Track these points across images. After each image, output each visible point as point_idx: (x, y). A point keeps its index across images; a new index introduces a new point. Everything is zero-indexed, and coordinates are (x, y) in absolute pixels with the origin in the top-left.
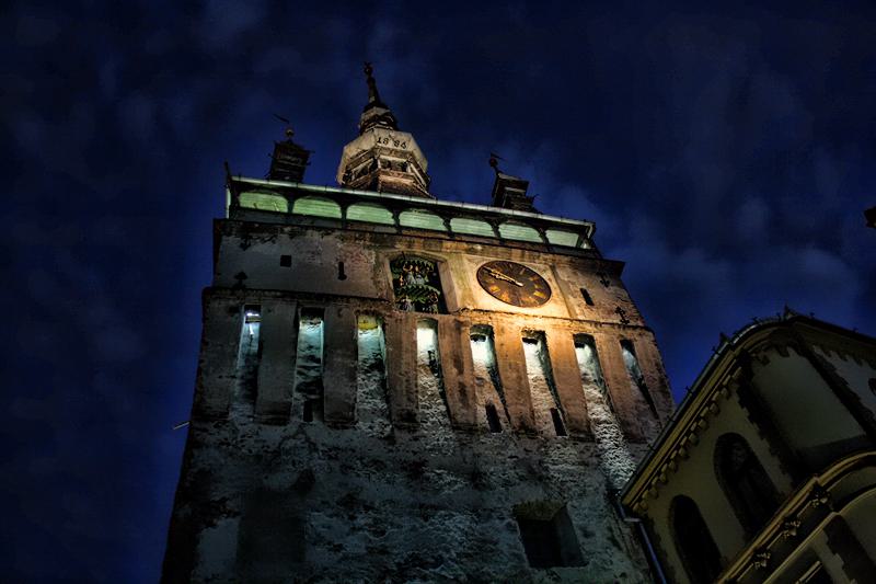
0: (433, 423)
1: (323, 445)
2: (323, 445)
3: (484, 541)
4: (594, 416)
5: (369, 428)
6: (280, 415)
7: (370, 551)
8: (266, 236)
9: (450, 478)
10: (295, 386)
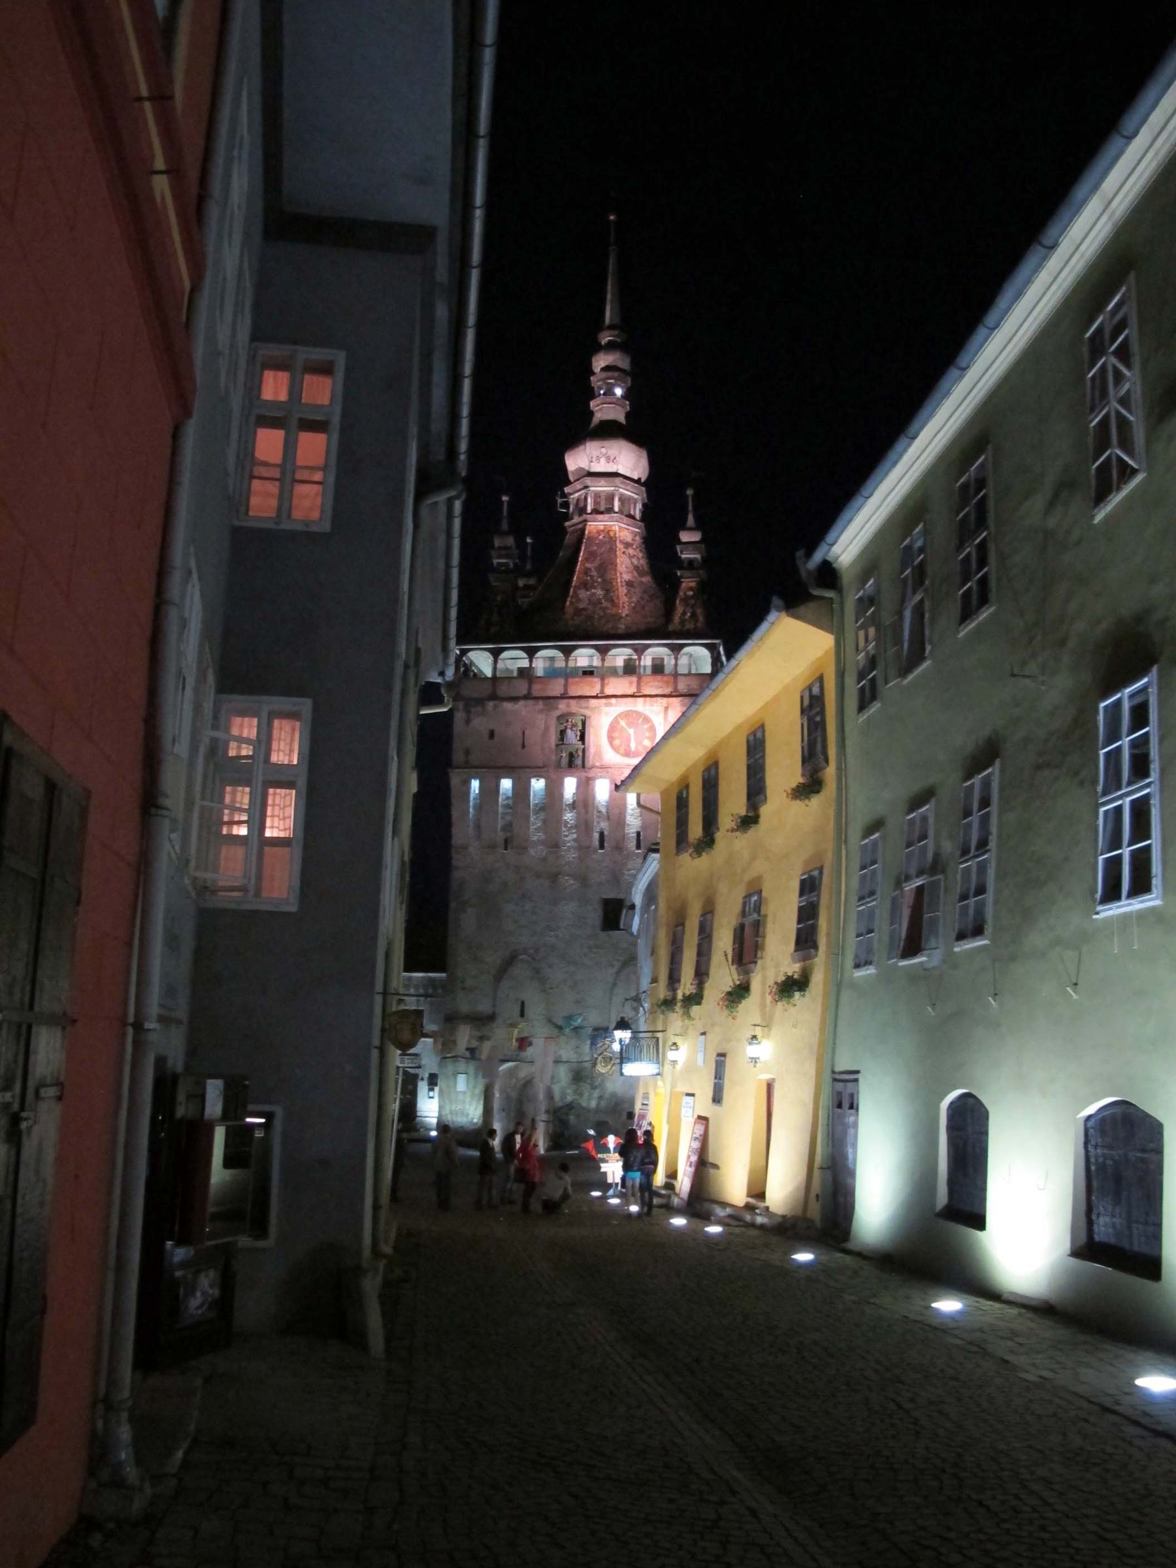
5: (536, 852)
8: (479, 709)
9: (572, 882)
10: (499, 829)
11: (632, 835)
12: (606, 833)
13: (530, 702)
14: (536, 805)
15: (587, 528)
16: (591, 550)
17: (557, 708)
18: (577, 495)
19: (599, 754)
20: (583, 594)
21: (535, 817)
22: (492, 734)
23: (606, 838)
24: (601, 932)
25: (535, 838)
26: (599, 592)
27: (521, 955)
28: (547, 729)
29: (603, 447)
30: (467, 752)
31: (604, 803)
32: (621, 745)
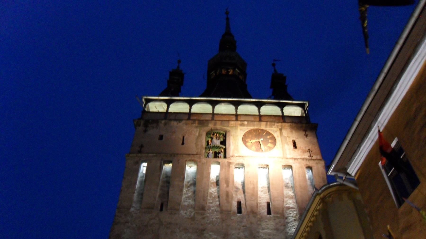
0: (212, 210)
4: (287, 205)
13: (190, 122)
14: (188, 182)
17: (208, 126)
21: (187, 189)
23: (243, 206)
25: (186, 204)
28: (200, 135)
30: (142, 146)
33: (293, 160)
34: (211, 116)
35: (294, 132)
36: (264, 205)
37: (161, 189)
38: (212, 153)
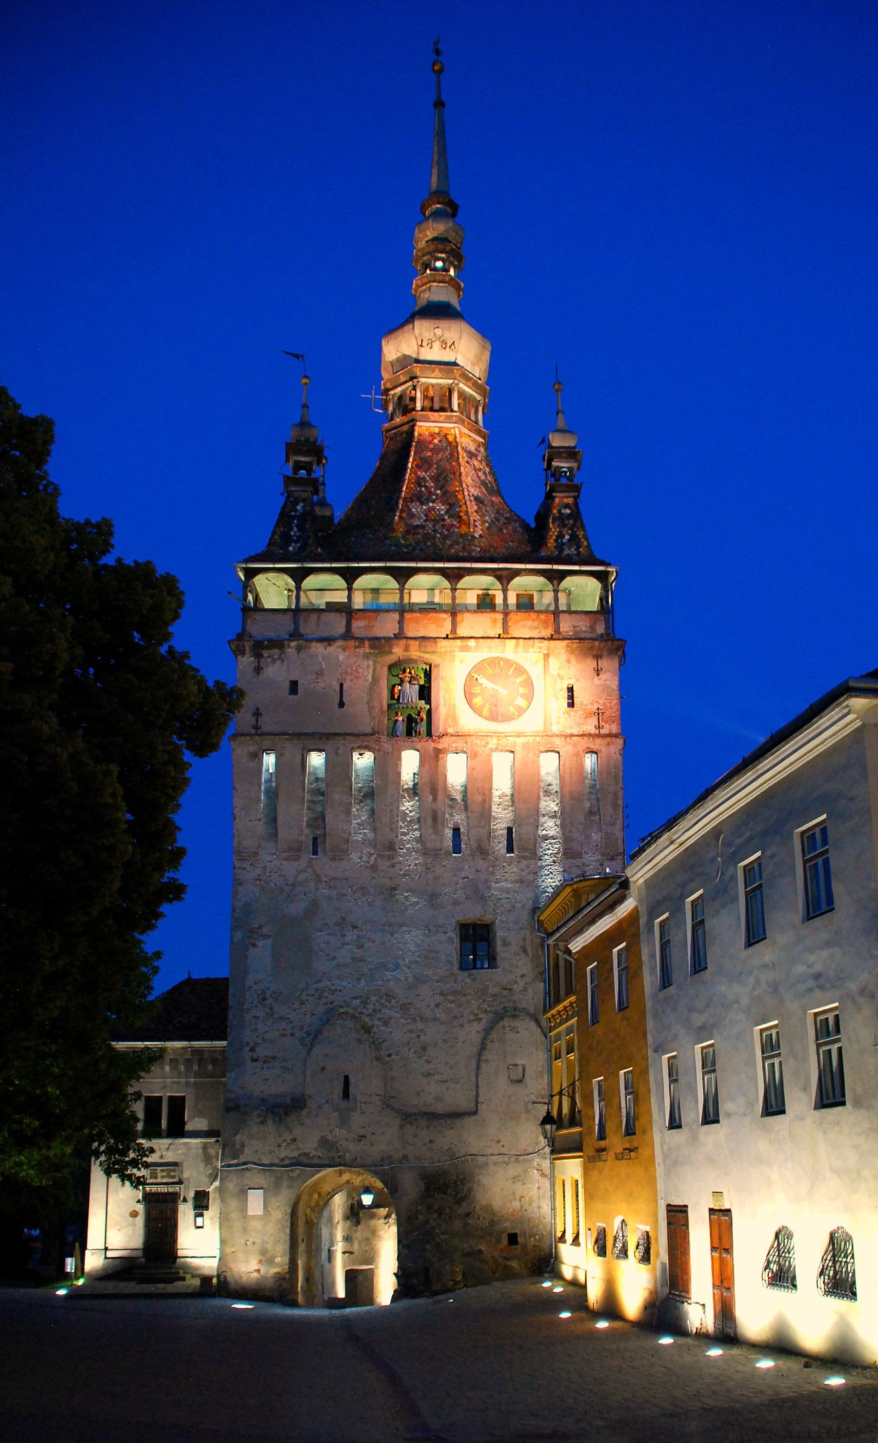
0: (408, 849)
1: (326, 876)
2: (326, 876)
3: (431, 951)
6: (294, 851)
7: (353, 959)
8: (276, 652)
11: (501, 832)
12: (462, 830)
13: (352, 643)
14: (360, 790)
15: (416, 428)
16: (422, 455)
18: (399, 390)
19: (453, 717)
20: (415, 508)
22: (294, 687)
24: (461, 972)
25: (359, 837)
26: (441, 508)
27: (342, 1007)
28: (375, 680)
29: (438, 327)
31: (459, 788)
32: (483, 706)
33: (563, 738)
34: (396, 616)
35: (573, 661)
36: (502, 835)
37: (309, 808)
38: (403, 720)
